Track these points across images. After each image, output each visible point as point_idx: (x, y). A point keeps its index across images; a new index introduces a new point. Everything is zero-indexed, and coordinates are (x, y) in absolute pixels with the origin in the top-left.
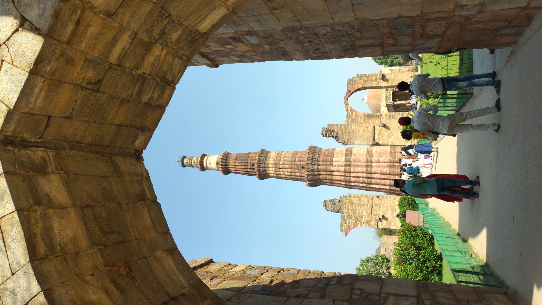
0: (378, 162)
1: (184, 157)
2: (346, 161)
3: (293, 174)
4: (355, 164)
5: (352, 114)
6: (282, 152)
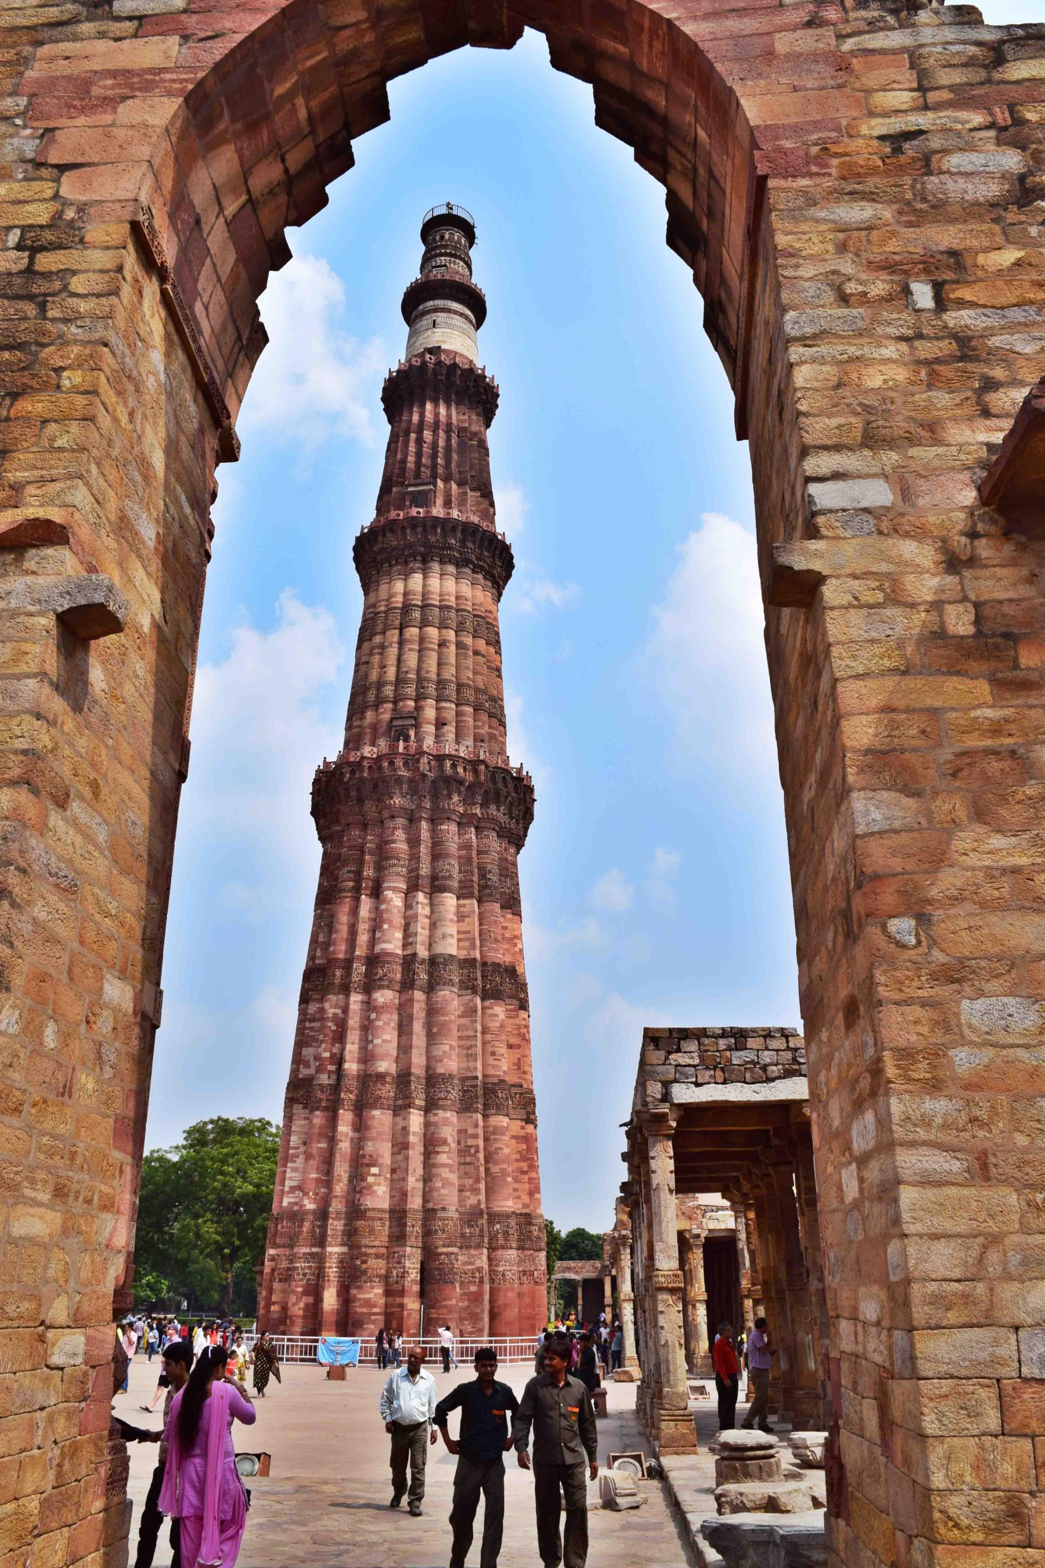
0: (431, 1144)
1: (468, 230)
2: (434, 962)
3: (371, 696)
4: (419, 1009)
6: (495, 642)
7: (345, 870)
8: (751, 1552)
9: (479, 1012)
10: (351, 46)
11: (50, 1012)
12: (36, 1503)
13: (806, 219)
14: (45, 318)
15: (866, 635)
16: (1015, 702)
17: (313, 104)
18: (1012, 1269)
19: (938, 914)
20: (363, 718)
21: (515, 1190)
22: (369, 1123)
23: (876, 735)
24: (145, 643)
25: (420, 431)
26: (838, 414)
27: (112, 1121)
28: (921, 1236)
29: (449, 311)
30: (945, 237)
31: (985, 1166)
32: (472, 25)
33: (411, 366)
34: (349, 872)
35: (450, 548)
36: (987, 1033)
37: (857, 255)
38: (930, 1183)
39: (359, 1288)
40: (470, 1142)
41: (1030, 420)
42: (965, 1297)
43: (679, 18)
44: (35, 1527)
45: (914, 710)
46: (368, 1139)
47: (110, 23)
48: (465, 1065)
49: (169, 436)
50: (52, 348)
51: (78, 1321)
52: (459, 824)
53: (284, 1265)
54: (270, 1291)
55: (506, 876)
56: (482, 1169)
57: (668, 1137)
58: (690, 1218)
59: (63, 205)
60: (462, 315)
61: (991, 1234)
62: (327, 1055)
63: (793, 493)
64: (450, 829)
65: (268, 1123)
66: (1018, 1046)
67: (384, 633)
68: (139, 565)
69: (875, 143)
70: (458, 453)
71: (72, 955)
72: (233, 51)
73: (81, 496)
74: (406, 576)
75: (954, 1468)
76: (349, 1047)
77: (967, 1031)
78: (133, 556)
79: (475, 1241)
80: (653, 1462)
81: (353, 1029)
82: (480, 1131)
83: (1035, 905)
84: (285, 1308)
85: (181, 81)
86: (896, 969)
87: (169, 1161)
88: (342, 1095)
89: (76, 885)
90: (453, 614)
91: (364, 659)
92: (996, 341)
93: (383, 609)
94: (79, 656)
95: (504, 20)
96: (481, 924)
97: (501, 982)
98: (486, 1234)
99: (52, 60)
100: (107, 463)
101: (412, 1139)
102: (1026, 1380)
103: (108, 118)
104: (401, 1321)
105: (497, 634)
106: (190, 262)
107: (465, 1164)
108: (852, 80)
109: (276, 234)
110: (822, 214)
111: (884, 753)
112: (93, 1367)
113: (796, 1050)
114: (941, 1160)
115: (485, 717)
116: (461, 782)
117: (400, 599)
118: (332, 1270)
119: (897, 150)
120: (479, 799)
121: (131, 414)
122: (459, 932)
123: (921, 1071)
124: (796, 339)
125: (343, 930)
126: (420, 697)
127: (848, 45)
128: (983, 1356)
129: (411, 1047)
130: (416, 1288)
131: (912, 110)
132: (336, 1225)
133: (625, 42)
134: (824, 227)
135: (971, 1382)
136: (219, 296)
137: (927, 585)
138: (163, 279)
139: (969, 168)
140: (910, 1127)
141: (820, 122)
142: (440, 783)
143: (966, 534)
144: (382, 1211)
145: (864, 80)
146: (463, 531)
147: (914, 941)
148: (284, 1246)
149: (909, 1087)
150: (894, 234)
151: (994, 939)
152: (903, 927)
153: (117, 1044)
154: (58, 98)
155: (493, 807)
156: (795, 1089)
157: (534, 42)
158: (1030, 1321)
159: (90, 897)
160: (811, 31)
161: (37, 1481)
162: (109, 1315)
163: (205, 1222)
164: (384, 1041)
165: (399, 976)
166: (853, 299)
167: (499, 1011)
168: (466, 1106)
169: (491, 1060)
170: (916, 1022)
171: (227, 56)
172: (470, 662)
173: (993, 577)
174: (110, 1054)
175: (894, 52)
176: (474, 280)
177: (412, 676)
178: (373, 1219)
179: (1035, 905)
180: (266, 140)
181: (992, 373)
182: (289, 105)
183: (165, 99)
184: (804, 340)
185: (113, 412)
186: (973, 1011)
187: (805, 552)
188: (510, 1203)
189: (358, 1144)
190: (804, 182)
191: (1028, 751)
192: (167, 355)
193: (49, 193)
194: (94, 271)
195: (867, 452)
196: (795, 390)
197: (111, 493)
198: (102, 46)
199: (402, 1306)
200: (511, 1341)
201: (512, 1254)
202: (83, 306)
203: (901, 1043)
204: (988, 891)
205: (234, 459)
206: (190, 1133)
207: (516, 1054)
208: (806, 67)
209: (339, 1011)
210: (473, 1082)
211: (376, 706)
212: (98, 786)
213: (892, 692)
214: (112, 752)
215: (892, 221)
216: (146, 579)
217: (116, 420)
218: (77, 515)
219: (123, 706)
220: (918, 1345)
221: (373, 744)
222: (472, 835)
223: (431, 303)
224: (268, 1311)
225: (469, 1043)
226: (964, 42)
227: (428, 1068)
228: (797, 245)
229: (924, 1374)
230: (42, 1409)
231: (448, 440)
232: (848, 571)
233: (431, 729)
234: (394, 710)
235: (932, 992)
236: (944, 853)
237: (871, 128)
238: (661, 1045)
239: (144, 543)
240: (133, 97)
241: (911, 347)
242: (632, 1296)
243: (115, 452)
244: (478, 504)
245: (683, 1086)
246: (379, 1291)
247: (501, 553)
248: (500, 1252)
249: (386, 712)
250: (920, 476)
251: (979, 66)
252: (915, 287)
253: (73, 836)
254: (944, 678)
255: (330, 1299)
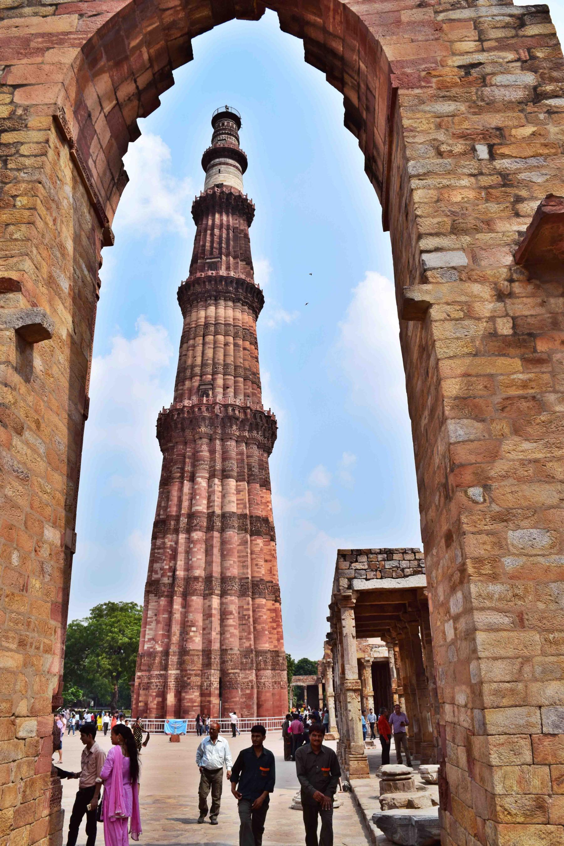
0: (224, 614)
1: (237, 120)
2: (224, 516)
3: (188, 373)
4: (216, 542)
6: (255, 343)
7: (175, 467)
8: (399, 830)
9: (249, 543)
10: (172, 19)
11: (15, 545)
12: (12, 812)
13: (419, 111)
14: (7, 169)
15: (454, 335)
16: (534, 370)
17: (152, 51)
18: (537, 675)
19: (495, 485)
20: (184, 385)
21: (270, 638)
22: (191, 603)
23: (460, 389)
24: (64, 345)
26: (438, 216)
27: (50, 604)
28: (488, 658)
29: (227, 164)
30: (494, 120)
31: (522, 620)
32: (237, 8)
33: (207, 194)
34: (178, 468)
35: (230, 292)
36: (522, 549)
37: (447, 130)
38: (492, 630)
39: (186, 692)
40: (245, 613)
41: (541, 218)
42: (512, 690)
43: (349, 3)
44: (11, 825)
45: (480, 375)
46: (191, 612)
47: (40, 8)
48: (241, 571)
49: (75, 232)
50: (10, 185)
51: (33, 713)
52: (237, 441)
53: (146, 680)
54: (138, 695)
55: (263, 469)
56: (252, 627)
57: (351, 608)
58: (364, 652)
59: (16, 107)
60: (234, 166)
61: (526, 657)
62: (167, 567)
63: (414, 259)
64: (232, 444)
65: (136, 604)
66: (539, 555)
67: (194, 339)
68: (60, 302)
69: (456, 70)
70: (233, 241)
71: (27, 514)
72: (107, 22)
73: (27, 265)
74: (206, 307)
75: (508, 783)
76: (179, 563)
77: (511, 548)
78: (57, 297)
79: (249, 666)
80: (346, 783)
81: (181, 553)
82: (251, 607)
83: (547, 479)
84: (146, 704)
85: (79, 39)
86: (472, 515)
87: (82, 626)
88: (176, 589)
89: (28, 477)
90: (231, 328)
91: (184, 353)
92: (522, 176)
93: (194, 326)
94: (28, 352)
95: (255, 4)
96: (249, 495)
97: (260, 527)
98: (254, 662)
99: (9, 27)
100: (41, 247)
101: (214, 612)
102: (546, 735)
103: (39, 59)
104: (209, 710)
105: (256, 338)
106: (85, 137)
107: (243, 624)
108: (443, 35)
109: (132, 122)
110: (428, 108)
111: (465, 399)
112: (42, 738)
113: (420, 560)
114: (498, 617)
115: (249, 383)
116: (237, 419)
117: (203, 320)
118: (172, 683)
119: (468, 74)
120: (247, 428)
121: (55, 220)
122: (237, 500)
123: (487, 569)
124: (414, 176)
125: (175, 500)
126: (214, 373)
127: (441, 17)
128: (522, 722)
129: (212, 562)
130: (217, 692)
131: (476, 51)
132: (173, 659)
133: (320, 16)
134: (429, 115)
135: (516, 736)
136: (102, 156)
137: (487, 307)
138: (71, 147)
139: (507, 83)
140: (481, 599)
141: (427, 58)
142: (226, 419)
143: (506, 280)
144: (198, 651)
145: (450, 36)
146: (236, 283)
147: (482, 500)
148: (145, 671)
149: (481, 578)
150: (466, 118)
151: (525, 497)
152: (476, 492)
153: (52, 563)
154: (12, 49)
155: (255, 432)
156: (419, 581)
157: (271, 17)
158: (547, 703)
159: (36, 483)
160: (420, 9)
161: (12, 800)
162: (50, 709)
163: (102, 659)
164: (198, 559)
165: (205, 524)
166: (445, 154)
167: (260, 542)
168: (242, 594)
169: (256, 569)
170: (484, 543)
171: (104, 25)
172: (241, 354)
173: (522, 303)
174: (48, 568)
175: (465, 20)
176: (241, 147)
177: (210, 362)
178: (193, 655)
179: (547, 479)
180: (126, 70)
181: (520, 193)
182: (138, 52)
183: (71, 49)
184: (419, 177)
185: (44, 218)
186: (514, 537)
187: (420, 291)
188: (267, 645)
189: (185, 615)
190: (417, 91)
191: (542, 397)
192: (74, 188)
193: (8, 100)
194: (33, 143)
195: (453, 237)
196: (414, 203)
197: (44, 263)
198: (36, 20)
199: (209, 702)
200: (269, 720)
201: (269, 673)
202: (27, 162)
203: (476, 554)
204: (522, 472)
205: (111, 244)
206: (93, 611)
207: (269, 565)
208: (418, 29)
209: (173, 543)
210: (246, 581)
211: (191, 379)
212: (39, 423)
213: (469, 366)
214: (46, 404)
215: (465, 112)
216: (64, 310)
217: (46, 224)
218: (25, 275)
219: (52, 379)
220: (487, 717)
221: (189, 399)
222: (243, 447)
223: (217, 160)
224: (137, 706)
225: (244, 559)
226: (503, 15)
227: (222, 573)
228: (415, 125)
229: (491, 732)
230: (14, 761)
231: (228, 234)
232: (444, 300)
233: (221, 390)
234: (201, 380)
235: (492, 527)
236: (497, 452)
237: (454, 62)
238: (347, 559)
239: (62, 290)
240: (53, 48)
241: (477, 180)
242: (333, 694)
243: (46, 241)
244: (245, 268)
245: (359, 580)
246: (197, 694)
247: (257, 294)
248: (262, 672)
249: (196, 382)
250: (482, 249)
251: (511, 27)
252: (478, 147)
253: (25, 449)
254: (496, 358)
255: (171, 699)
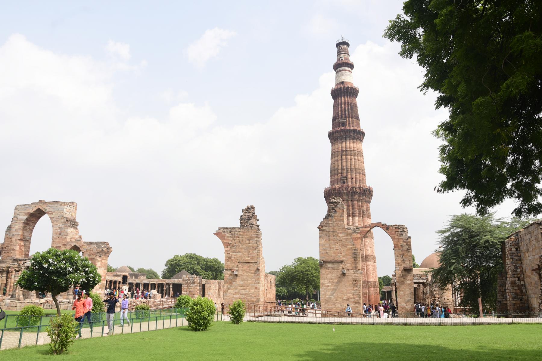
1: (348, 45)
3: (336, 172)
5: (358, 233)
6: (362, 156)
25: (341, 105)
29: (345, 70)
126: (347, 173)
167: (368, 240)
201: (373, 289)
207: (371, 249)
223: (341, 69)
231: (348, 107)
249: (339, 176)
